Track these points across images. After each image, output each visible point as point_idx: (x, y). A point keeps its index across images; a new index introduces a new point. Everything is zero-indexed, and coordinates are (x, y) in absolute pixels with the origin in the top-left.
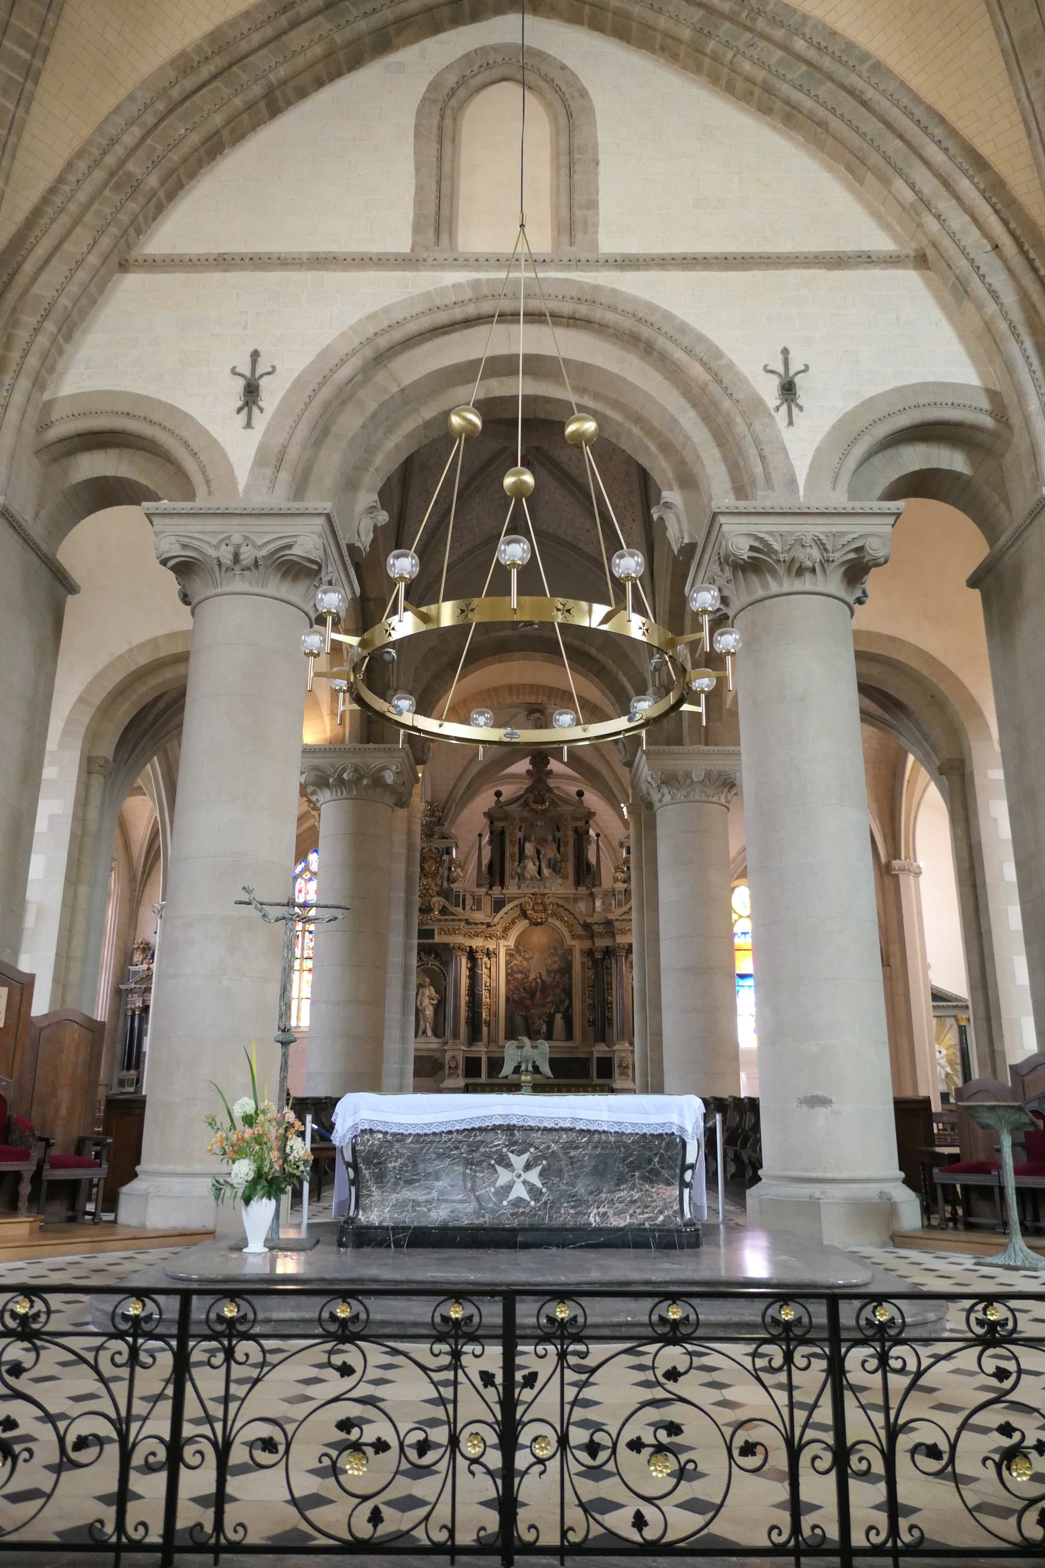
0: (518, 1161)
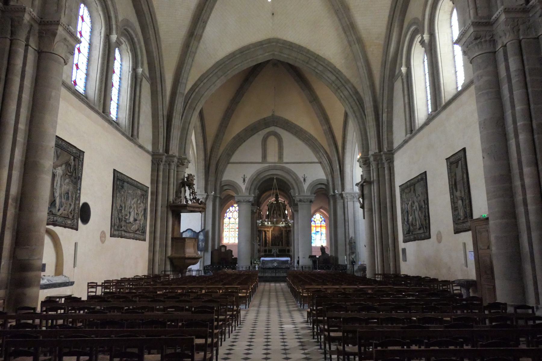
0: (275, 263)
